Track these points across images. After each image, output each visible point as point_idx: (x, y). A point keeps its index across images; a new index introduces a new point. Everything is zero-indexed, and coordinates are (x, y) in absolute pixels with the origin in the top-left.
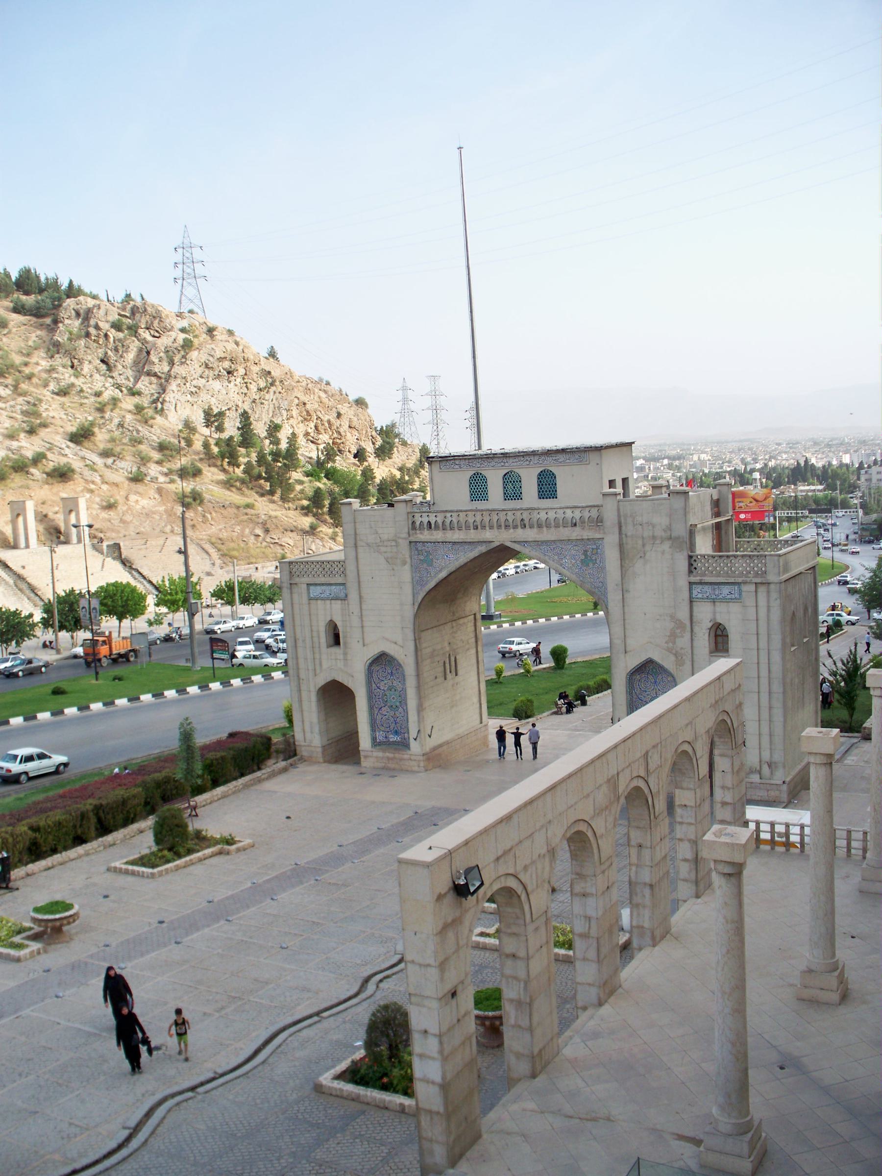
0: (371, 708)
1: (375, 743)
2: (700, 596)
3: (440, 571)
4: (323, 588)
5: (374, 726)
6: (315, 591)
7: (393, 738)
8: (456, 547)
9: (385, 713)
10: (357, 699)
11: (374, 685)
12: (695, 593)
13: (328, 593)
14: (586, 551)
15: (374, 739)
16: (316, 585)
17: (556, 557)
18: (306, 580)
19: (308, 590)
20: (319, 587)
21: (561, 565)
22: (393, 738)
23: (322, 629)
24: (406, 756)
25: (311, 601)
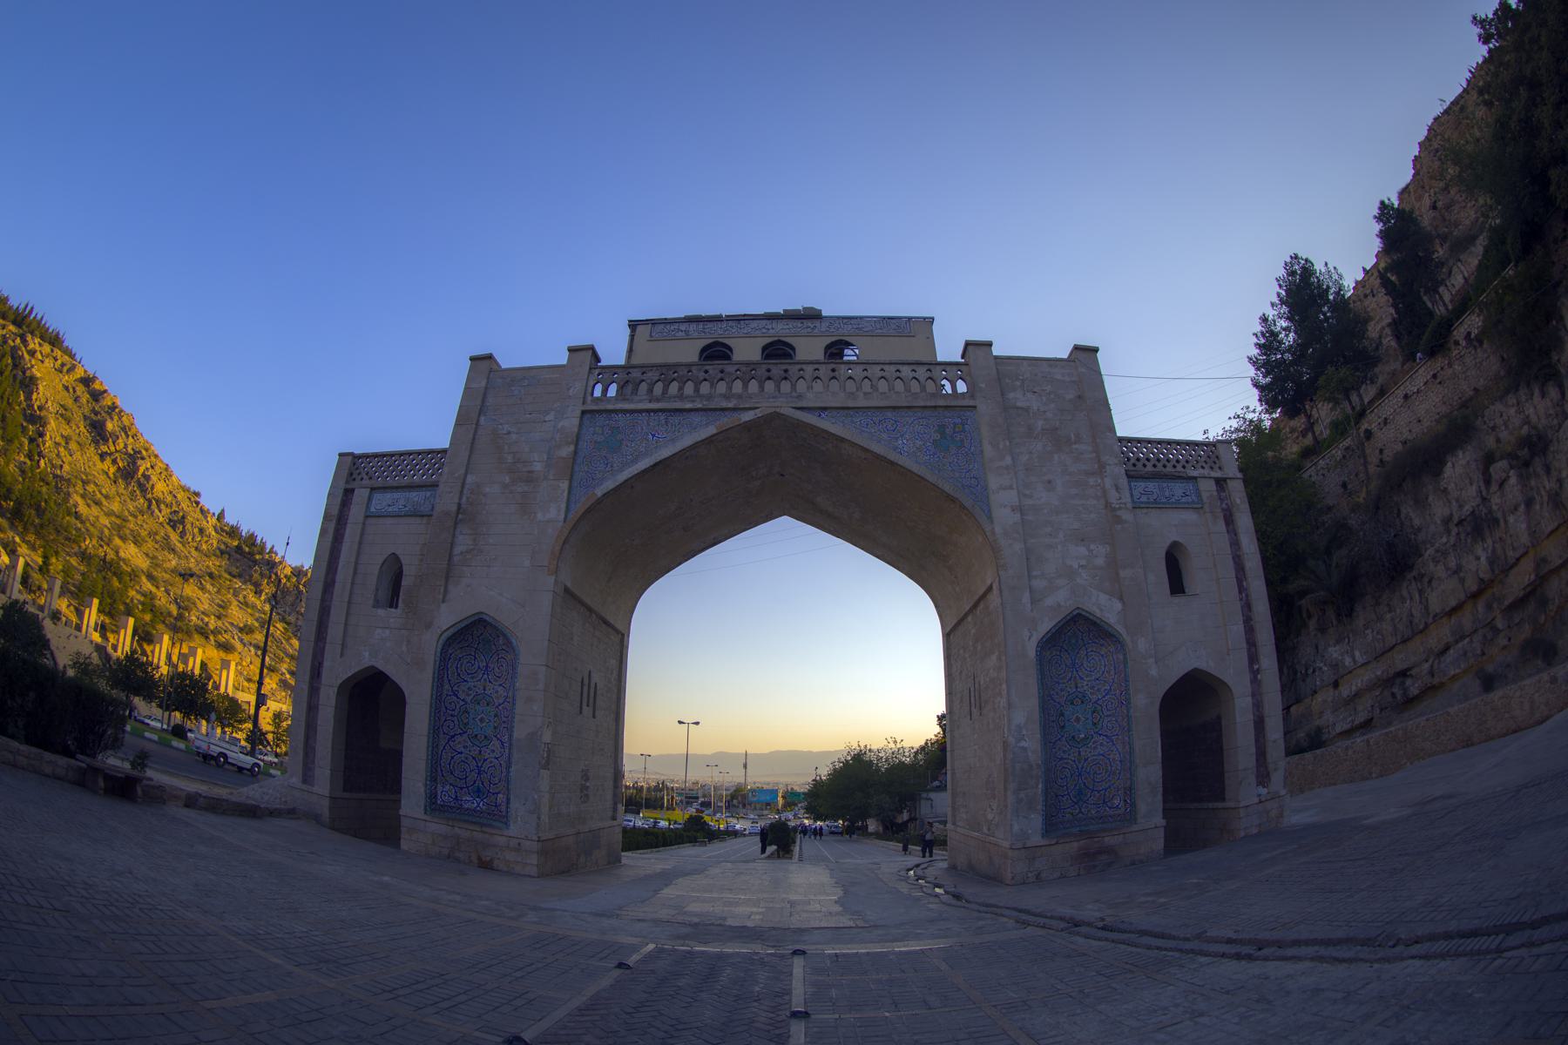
0: (435, 730)
1: (433, 805)
2: (1144, 499)
3: (635, 461)
4: (396, 495)
5: (435, 773)
6: (382, 501)
7: (470, 802)
8: (675, 419)
9: (460, 748)
10: (410, 710)
11: (447, 686)
12: (1136, 493)
13: (402, 502)
14: (942, 429)
15: (432, 797)
16: (385, 489)
17: (885, 436)
18: (373, 483)
19: (370, 499)
20: (388, 495)
21: (895, 449)
22: (470, 802)
23: (376, 570)
24: (502, 840)
25: (370, 521)
